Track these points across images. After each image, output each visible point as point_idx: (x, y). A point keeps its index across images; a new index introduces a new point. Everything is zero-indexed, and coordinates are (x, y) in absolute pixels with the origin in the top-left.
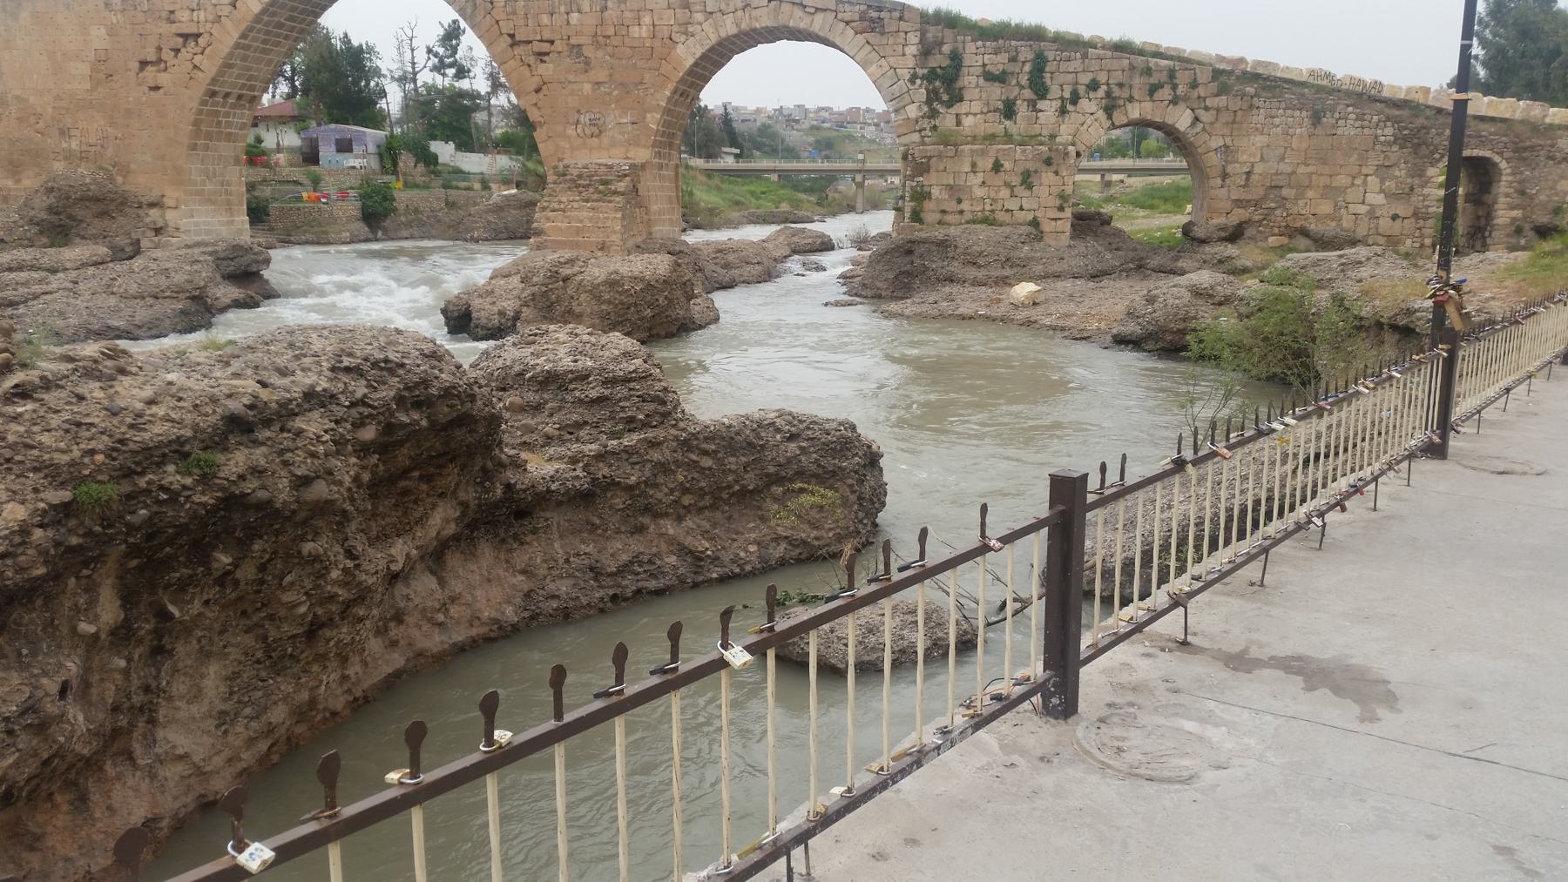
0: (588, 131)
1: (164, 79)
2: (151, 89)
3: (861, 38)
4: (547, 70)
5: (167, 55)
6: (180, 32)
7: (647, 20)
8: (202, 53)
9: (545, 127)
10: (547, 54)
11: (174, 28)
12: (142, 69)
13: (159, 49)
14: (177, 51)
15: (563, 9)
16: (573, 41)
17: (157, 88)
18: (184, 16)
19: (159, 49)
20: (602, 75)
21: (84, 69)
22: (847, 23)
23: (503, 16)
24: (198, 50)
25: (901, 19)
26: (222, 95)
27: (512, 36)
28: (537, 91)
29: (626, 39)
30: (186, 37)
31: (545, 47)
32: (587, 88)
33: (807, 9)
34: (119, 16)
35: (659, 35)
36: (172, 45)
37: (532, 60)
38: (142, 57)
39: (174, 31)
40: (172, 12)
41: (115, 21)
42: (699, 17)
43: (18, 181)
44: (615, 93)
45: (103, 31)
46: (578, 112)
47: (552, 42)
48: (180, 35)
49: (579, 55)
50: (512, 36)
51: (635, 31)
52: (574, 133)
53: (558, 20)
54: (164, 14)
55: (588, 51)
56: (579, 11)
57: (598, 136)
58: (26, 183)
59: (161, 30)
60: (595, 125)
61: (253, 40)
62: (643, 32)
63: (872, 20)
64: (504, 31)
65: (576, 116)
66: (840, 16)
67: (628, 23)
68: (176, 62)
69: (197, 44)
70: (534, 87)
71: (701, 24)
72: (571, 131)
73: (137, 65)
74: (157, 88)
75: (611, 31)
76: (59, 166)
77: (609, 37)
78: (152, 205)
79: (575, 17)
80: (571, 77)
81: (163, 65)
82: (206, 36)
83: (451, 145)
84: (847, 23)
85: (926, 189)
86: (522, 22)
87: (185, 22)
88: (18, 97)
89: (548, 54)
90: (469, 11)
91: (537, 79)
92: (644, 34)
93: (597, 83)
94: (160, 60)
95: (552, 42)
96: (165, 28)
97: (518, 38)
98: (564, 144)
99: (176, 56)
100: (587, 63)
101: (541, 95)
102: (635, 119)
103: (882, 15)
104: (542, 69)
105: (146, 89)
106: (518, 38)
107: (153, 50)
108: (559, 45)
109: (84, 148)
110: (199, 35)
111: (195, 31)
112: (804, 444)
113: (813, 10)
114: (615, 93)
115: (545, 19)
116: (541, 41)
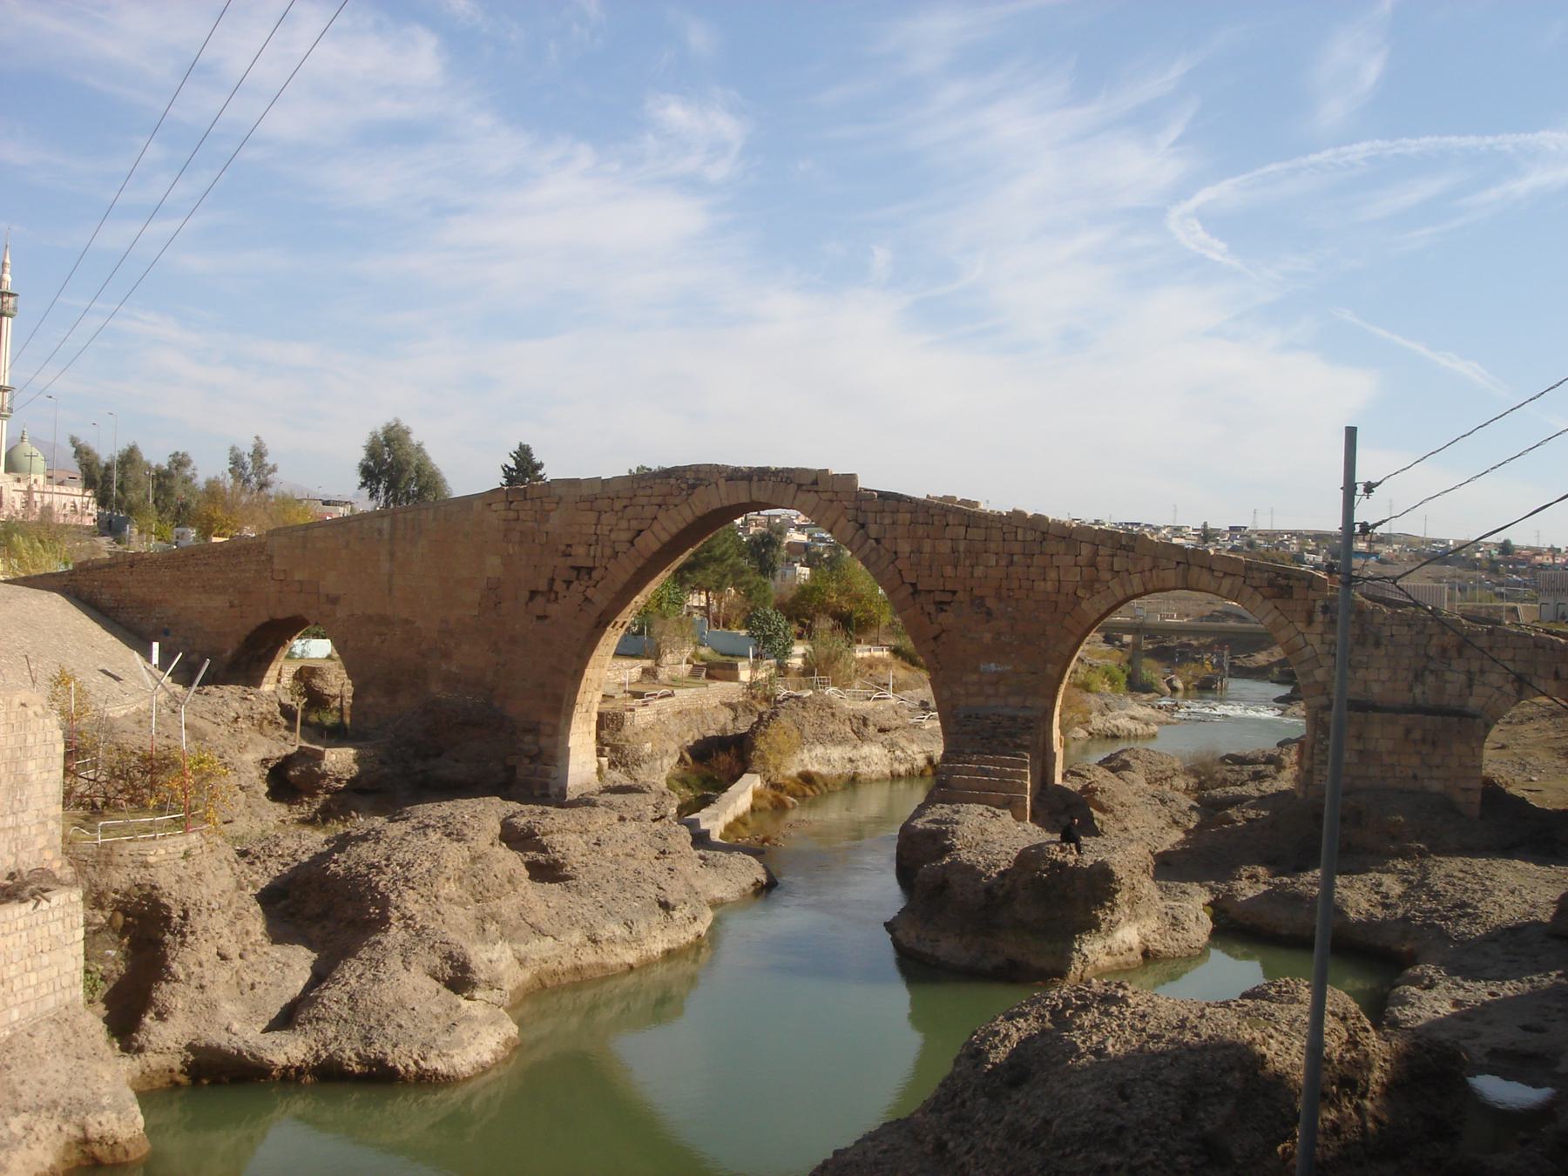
1: (553, 609)
2: (539, 617)
3: (1269, 605)
4: (947, 618)
5: (559, 586)
7: (1053, 574)
8: (595, 587)
11: (570, 562)
13: (552, 580)
14: (569, 583)
15: (968, 562)
16: (976, 592)
17: (545, 617)
18: (580, 550)
19: (552, 580)
22: (1256, 588)
24: (592, 583)
25: (1309, 587)
28: (935, 638)
30: (578, 569)
31: (947, 597)
32: (988, 637)
33: (1215, 573)
34: (516, 547)
37: (932, 609)
40: (569, 546)
41: (511, 551)
42: (1107, 576)
44: (1015, 643)
48: (573, 568)
50: (914, 585)
51: (1040, 585)
55: (991, 603)
62: (1049, 586)
66: (1248, 581)
69: (590, 578)
71: (1108, 582)
73: (527, 594)
78: (528, 731)
79: (979, 571)
84: (1256, 588)
87: (581, 555)
88: (406, 621)
95: (954, 593)
97: (919, 587)
99: (568, 588)
103: (1291, 583)
105: (535, 619)
108: (960, 595)
111: (591, 565)
113: (1221, 575)
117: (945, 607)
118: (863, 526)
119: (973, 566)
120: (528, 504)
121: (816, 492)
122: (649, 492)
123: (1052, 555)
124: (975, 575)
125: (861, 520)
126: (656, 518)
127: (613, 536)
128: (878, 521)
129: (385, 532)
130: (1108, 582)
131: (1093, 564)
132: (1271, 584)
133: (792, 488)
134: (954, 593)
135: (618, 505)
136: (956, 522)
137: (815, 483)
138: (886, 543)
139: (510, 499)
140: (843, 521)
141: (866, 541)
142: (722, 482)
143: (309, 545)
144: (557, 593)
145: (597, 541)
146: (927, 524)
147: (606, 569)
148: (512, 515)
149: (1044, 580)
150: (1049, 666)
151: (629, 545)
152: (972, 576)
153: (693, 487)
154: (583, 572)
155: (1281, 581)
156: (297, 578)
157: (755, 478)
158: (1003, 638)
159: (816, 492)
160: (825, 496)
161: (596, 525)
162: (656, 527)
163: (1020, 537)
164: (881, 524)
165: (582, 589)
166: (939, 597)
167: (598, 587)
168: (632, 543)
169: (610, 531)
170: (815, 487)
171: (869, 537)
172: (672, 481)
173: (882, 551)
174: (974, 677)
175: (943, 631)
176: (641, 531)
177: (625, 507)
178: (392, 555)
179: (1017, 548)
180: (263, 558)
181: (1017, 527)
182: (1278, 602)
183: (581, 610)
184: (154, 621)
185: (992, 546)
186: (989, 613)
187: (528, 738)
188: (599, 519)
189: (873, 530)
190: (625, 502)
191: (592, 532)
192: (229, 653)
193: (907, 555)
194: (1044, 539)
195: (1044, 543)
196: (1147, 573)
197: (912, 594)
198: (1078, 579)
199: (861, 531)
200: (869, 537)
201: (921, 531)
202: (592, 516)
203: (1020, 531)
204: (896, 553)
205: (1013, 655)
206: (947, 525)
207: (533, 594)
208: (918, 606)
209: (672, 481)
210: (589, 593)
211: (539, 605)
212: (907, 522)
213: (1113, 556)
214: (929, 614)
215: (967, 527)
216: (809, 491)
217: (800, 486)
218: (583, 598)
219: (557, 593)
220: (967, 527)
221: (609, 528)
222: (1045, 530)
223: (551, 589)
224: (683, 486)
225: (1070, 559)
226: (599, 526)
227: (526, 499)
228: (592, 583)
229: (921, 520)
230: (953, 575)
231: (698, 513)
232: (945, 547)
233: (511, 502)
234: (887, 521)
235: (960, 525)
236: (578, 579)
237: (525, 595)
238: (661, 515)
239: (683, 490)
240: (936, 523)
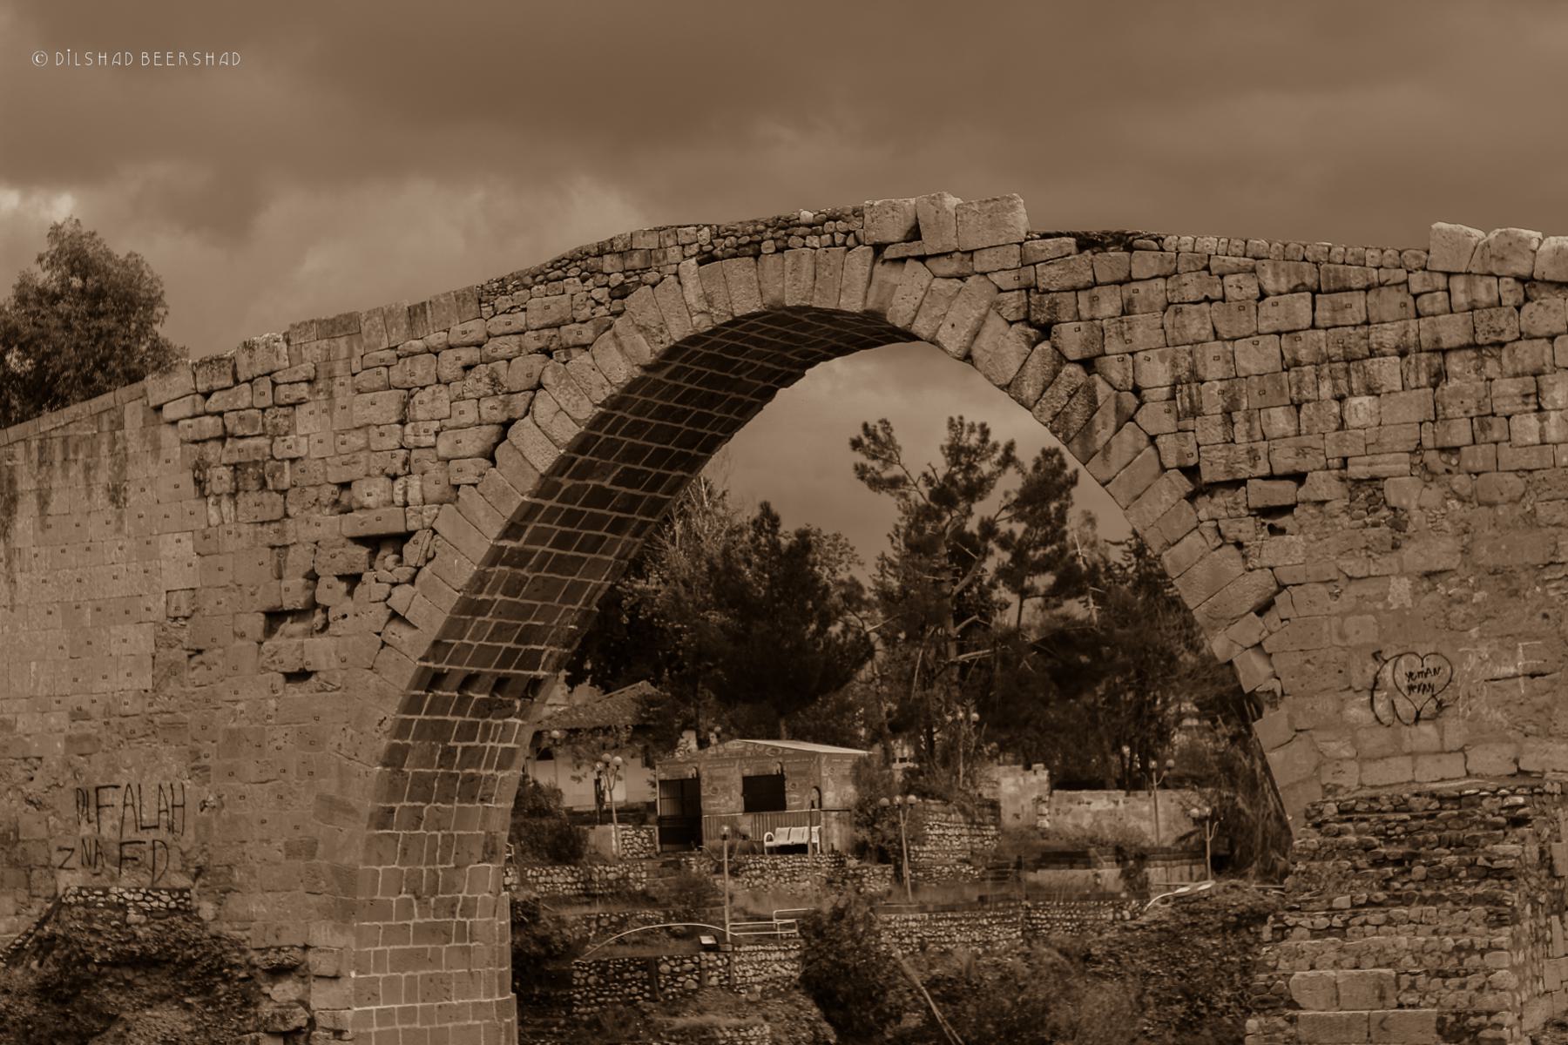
0: (1405, 707)
1: (320, 651)
2: (290, 677)
5: (331, 592)
6: (362, 531)
8: (412, 581)
9: (1283, 709)
10: (1287, 510)
13: (313, 577)
14: (353, 580)
15: (1326, 389)
18: (371, 492)
19: (313, 577)
20: (1441, 552)
21: (141, 640)
23: (1168, 423)
24: (404, 573)
26: (458, 680)
27: (1191, 472)
28: (1262, 609)
30: (374, 543)
31: (1282, 492)
32: (1400, 590)
34: (226, 505)
36: (341, 566)
37: (1246, 528)
38: (271, 602)
39: (349, 531)
40: (345, 486)
45: (188, 545)
46: (1376, 656)
47: (1299, 478)
48: (360, 540)
52: (1365, 716)
54: (327, 493)
56: (1371, 391)
57: (1432, 719)
59: (317, 533)
60: (1424, 688)
61: (536, 538)
64: (1171, 460)
65: (1371, 667)
67: (1508, 409)
68: (348, 606)
69: (400, 561)
70: (1252, 600)
72: (1356, 711)
73: (260, 621)
74: (300, 676)
75: (1460, 433)
76: (70, 881)
77: (1455, 450)
78: (279, 972)
80: (1353, 566)
81: (319, 618)
82: (423, 538)
83: (1040, 776)
86: (1217, 434)
89: (1287, 510)
90: (1077, 419)
91: (1262, 579)
93: (1429, 575)
94: (313, 606)
96: (330, 526)
97: (1206, 477)
98: (1338, 747)
99: (350, 593)
100: (1398, 525)
101: (1272, 618)
102: (1534, 664)
104: (1272, 551)
105: (279, 680)
106: (1206, 477)
109: (130, 834)
110: (405, 537)
114: (1478, 596)
116: (1271, 477)
117: (1280, 522)
119: (1340, 399)
120: (244, 395)
121: (922, 259)
122: (519, 320)
123: (1552, 338)
124: (1352, 421)
125: (1043, 317)
126: (540, 386)
128: (1085, 314)
134: (1299, 478)
136: (1283, 287)
137: (914, 234)
139: (202, 387)
141: (1056, 373)
144: (326, 610)
145: (406, 462)
146: (1208, 300)
147: (435, 532)
148: (210, 425)
149: (1540, 409)
151: (485, 463)
152: (1342, 425)
153: (621, 292)
157: (768, 246)
158: (1441, 588)
159: (922, 259)
161: (403, 423)
162: (543, 406)
163: (1460, 298)
164: (1092, 319)
165: (381, 591)
166: (1263, 493)
167: (421, 578)
169: (437, 434)
170: (915, 249)
171: (1062, 359)
172: (573, 285)
173: (1102, 390)
175: (1282, 587)
176: (507, 425)
181: (1448, 275)
183: (384, 644)
187: (285, 991)
188: (406, 405)
189: (1071, 338)
190: (468, 355)
194: (1527, 299)
195: (1527, 309)
199: (1044, 346)
201: (1195, 324)
202: (389, 403)
203: (1458, 284)
204: (1137, 390)
205: (1474, 632)
206: (1263, 295)
207: (275, 617)
209: (573, 285)
211: (292, 643)
214: (1239, 545)
215: (1315, 292)
216: (903, 260)
217: (879, 248)
218: (384, 615)
220: (1315, 292)
221: (436, 425)
222: (1523, 269)
226: (408, 428)
227: (237, 382)
229: (1192, 293)
230: (1291, 429)
232: (1256, 358)
235: (1294, 290)
239: (598, 303)
240: (1233, 293)
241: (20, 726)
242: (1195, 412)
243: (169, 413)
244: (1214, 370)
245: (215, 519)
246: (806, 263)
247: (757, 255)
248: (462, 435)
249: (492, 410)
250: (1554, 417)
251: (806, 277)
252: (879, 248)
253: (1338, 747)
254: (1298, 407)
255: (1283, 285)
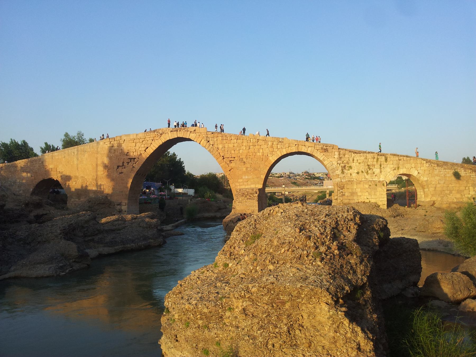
1: (124, 170)
2: (120, 173)
3: (322, 154)
4: (233, 165)
7: (261, 151)
8: (135, 163)
11: (128, 157)
12: (118, 168)
16: (241, 157)
19: (124, 162)
24: (135, 162)
28: (230, 170)
29: (256, 156)
30: (131, 159)
31: (233, 159)
32: (244, 169)
34: (113, 154)
35: (264, 155)
36: (127, 161)
41: (111, 156)
43: (79, 199)
44: (252, 170)
48: (129, 159)
49: (242, 160)
51: (258, 154)
53: (236, 152)
55: (245, 160)
58: (82, 200)
59: (124, 158)
62: (261, 154)
63: (325, 149)
67: (255, 152)
68: (128, 166)
71: (276, 152)
73: (117, 167)
78: (118, 205)
79: (241, 151)
81: (124, 167)
85: (344, 193)
86: (227, 153)
92: (260, 155)
96: (125, 157)
97: (225, 157)
98: (237, 184)
99: (128, 164)
107: (121, 163)
108: (236, 158)
112: (409, 244)
115: (233, 152)
118: (209, 141)
122: (149, 136)
127: (140, 149)
129: (75, 152)
130: (276, 152)
131: (272, 147)
132: (322, 149)
133: (189, 132)
135: (141, 141)
138: (216, 146)
139: (110, 141)
140: (203, 140)
142: (169, 132)
143: (54, 158)
144: (125, 166)
150: (262, 176)
153: (162, 134)
154: (132, 160)
155: (325, 147)
156: (50, 167)
157: (178, 131)
160: (198, 134)
165: (132, 164)
167: (137, 163)
168: (145, 151)
170: (195, 132)
171: (210, 144)
173: (214, 148)
174: (241, 180)
176: (148, 147)
177: (143, 141)
178: (78, 159)
179: (251, 144)
180: (40, 162)
182: (324, 153)
184: (9, 182)
185: (244, 144)
186: (244, 163)
187: (119, 207)
189: (211, 142)
190: (143, 140)
191: (134, 148)
192: (31, 190)
193: (221, 148)
196: (287, 148)
197: (223, 159)
198: (268, 151)
200: (210, 144)
202: (134, 144)
203: (251, 139)
204: (218, 148)
208: (225, 162)
209: (156, 133)
210: (134, 165)
212: (221, 139)
213: (277, 144)
217: (191, 132)
219: (125, 166)
222: (258, 139)
223: (123, 165)
224: (159, 134)
225: (266, 146)
228: (135, 162)
231: (163, 142)
232: (231, 145)
233: (111, 142)
234: (215, 140)
236: (130, 162)
237: (116, 167)
238: (153, 142)
241: (85, 177)
242: (224, 151)
243: (106, 143)
244: (226, 146)
245: (111, 156)
246: (183, 133)
247: (177, 131)
248: (142, 148)
249: (146, 146)
250: (261, 153)
251: (183, 134)
252: (191, 132)
253: (237, 184)
254: (235, 151)
255: (234, 138)
